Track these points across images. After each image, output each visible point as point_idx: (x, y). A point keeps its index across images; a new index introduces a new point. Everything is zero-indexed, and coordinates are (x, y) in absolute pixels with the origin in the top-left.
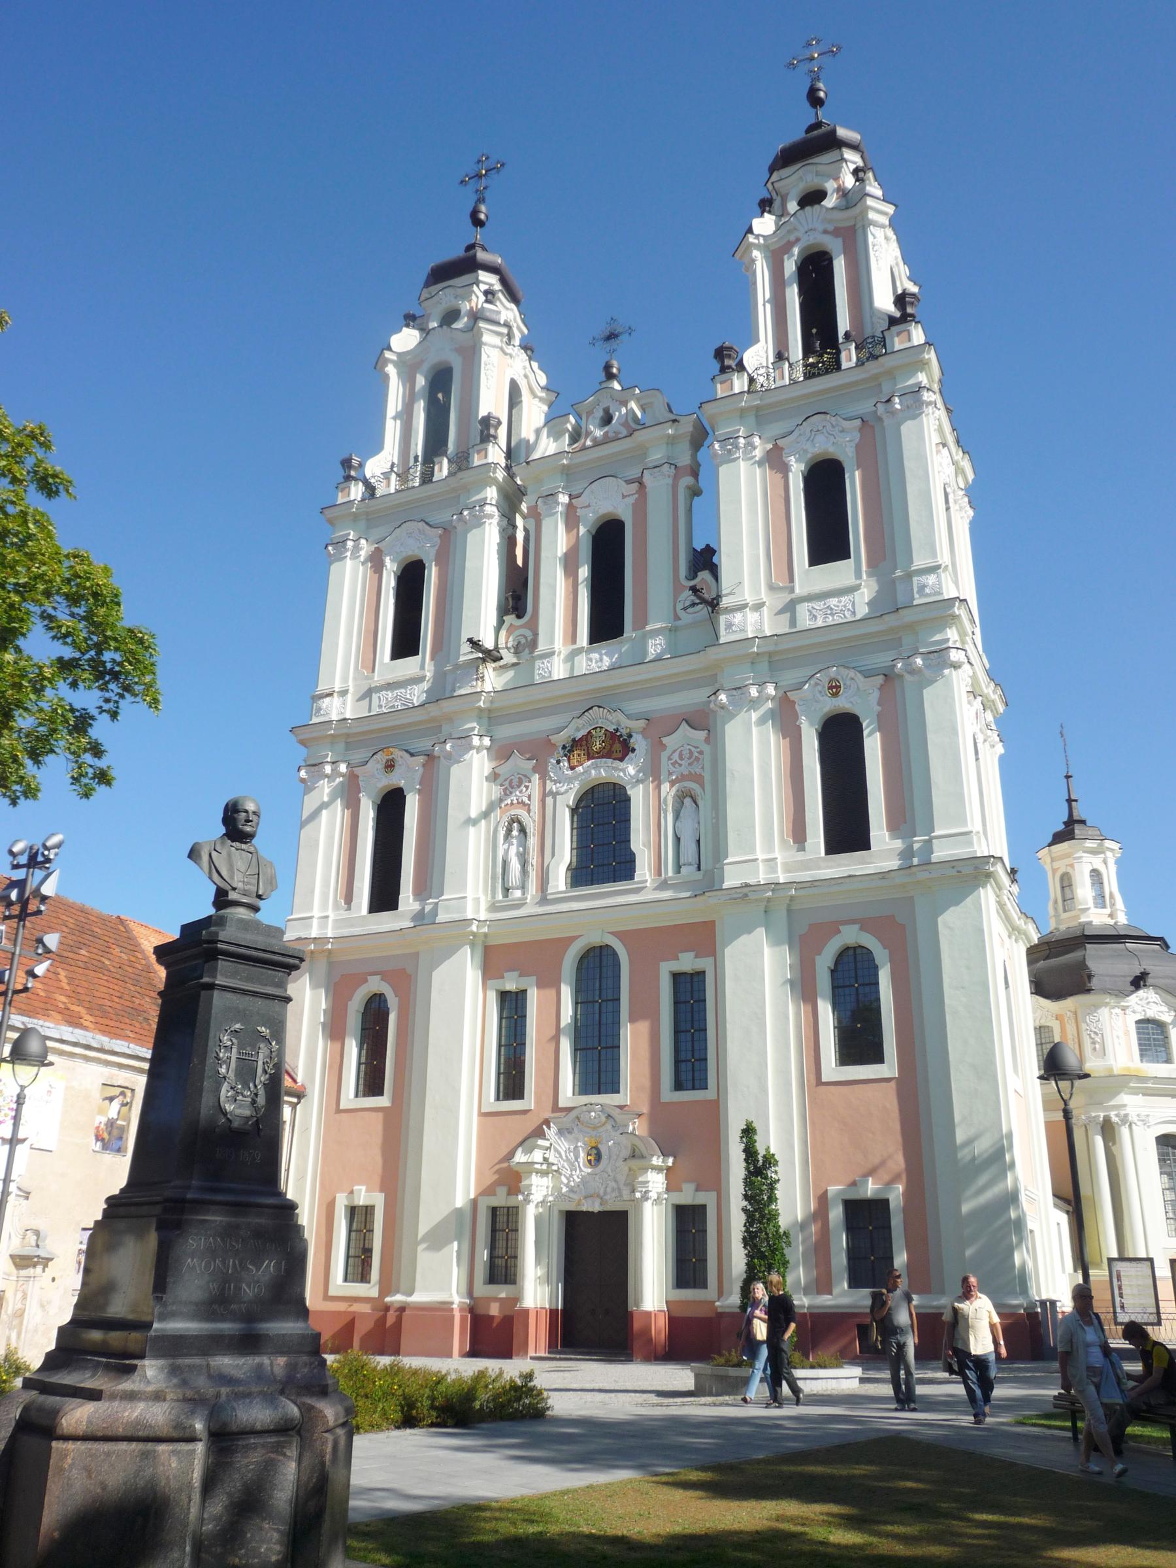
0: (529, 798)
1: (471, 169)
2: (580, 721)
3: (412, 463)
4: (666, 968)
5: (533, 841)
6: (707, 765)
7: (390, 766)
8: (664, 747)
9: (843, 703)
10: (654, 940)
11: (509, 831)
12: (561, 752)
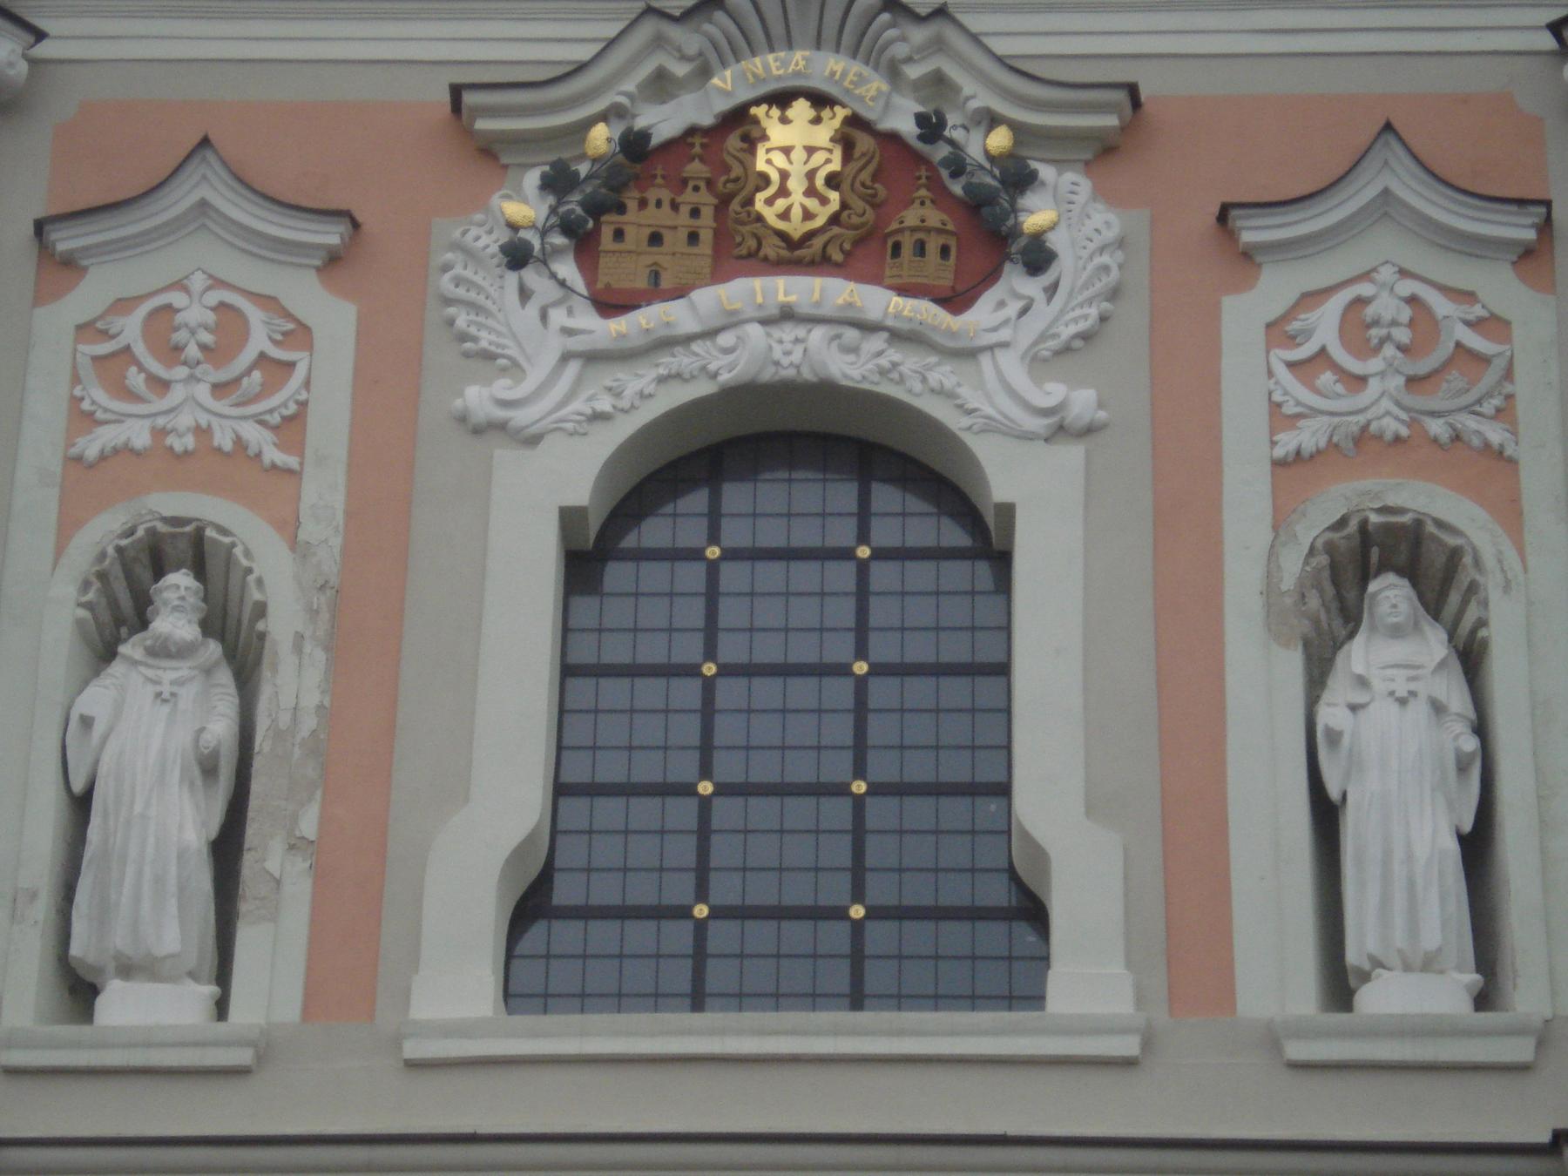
0: (291, 428)
2: (689, 39)
5: (295, 686)
12: (524, 205)
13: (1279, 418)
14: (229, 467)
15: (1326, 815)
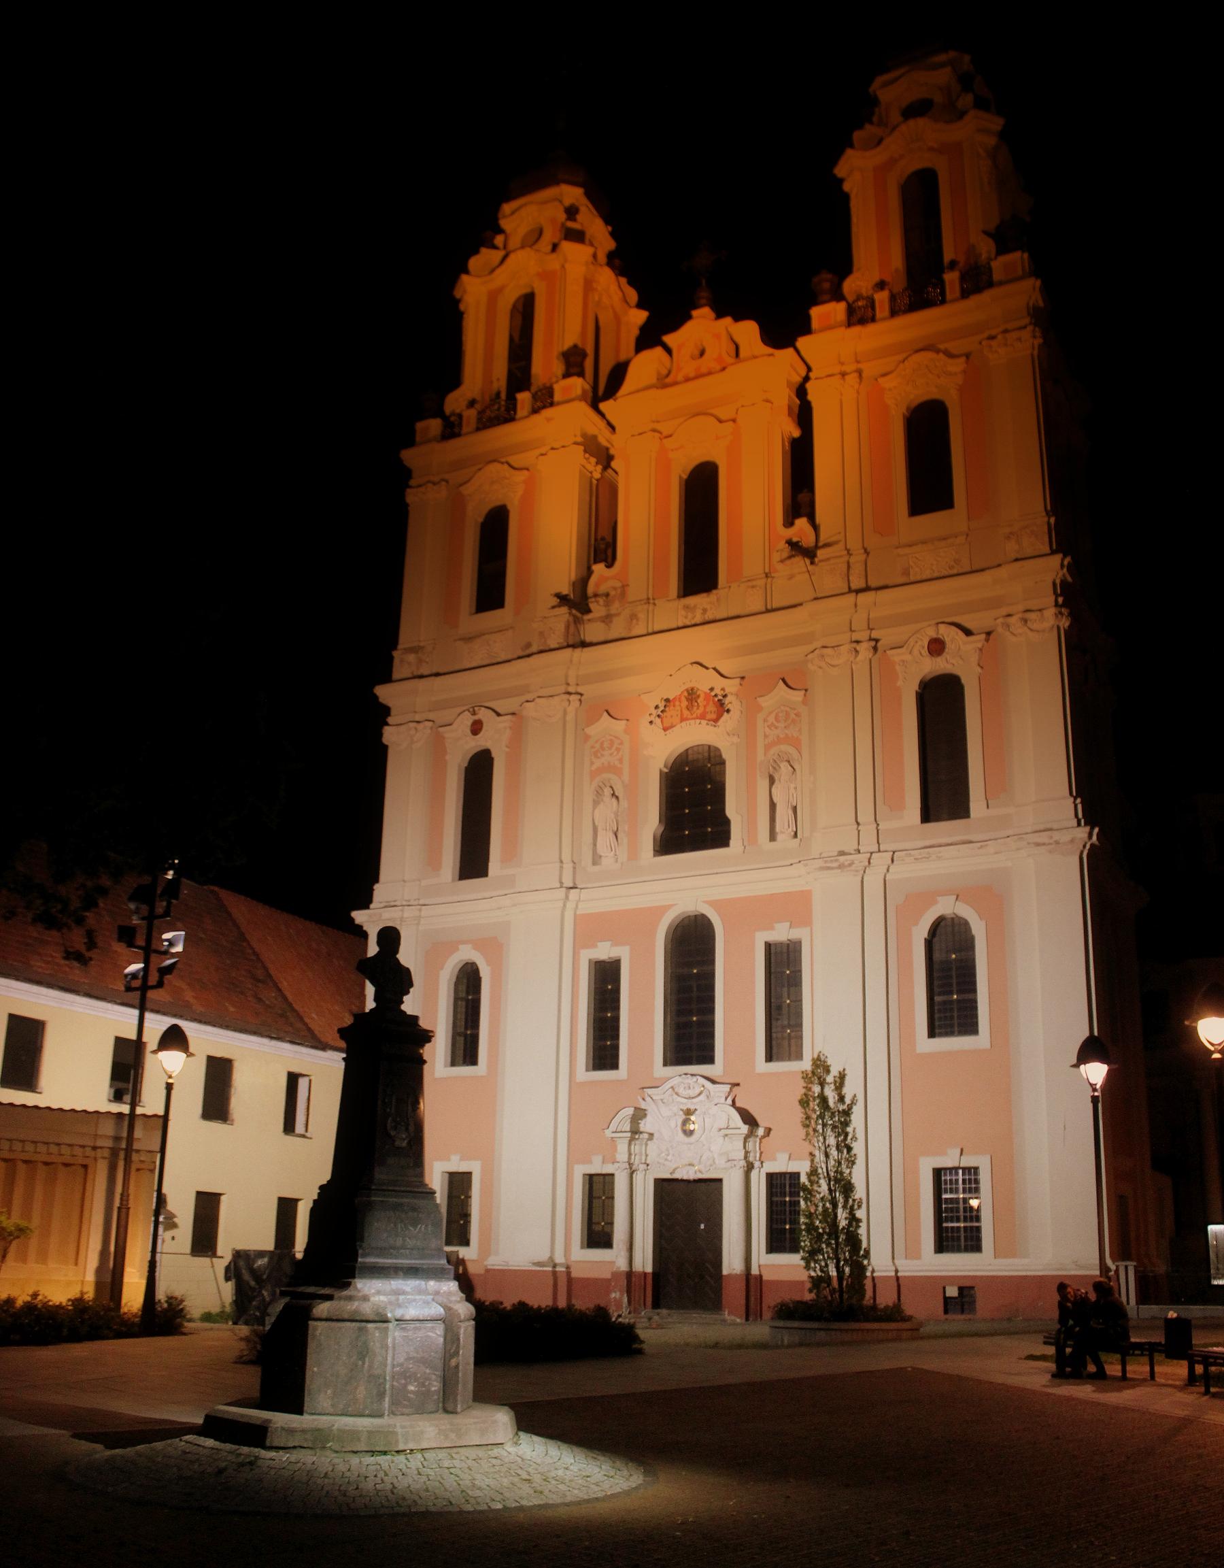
0: (621, 760)
4: (762, 938)
5: (624, 803)
7: (476, 728)
8: (760, 709)
13: (766, 736)
14: (610, 768)
15: (773, 806)
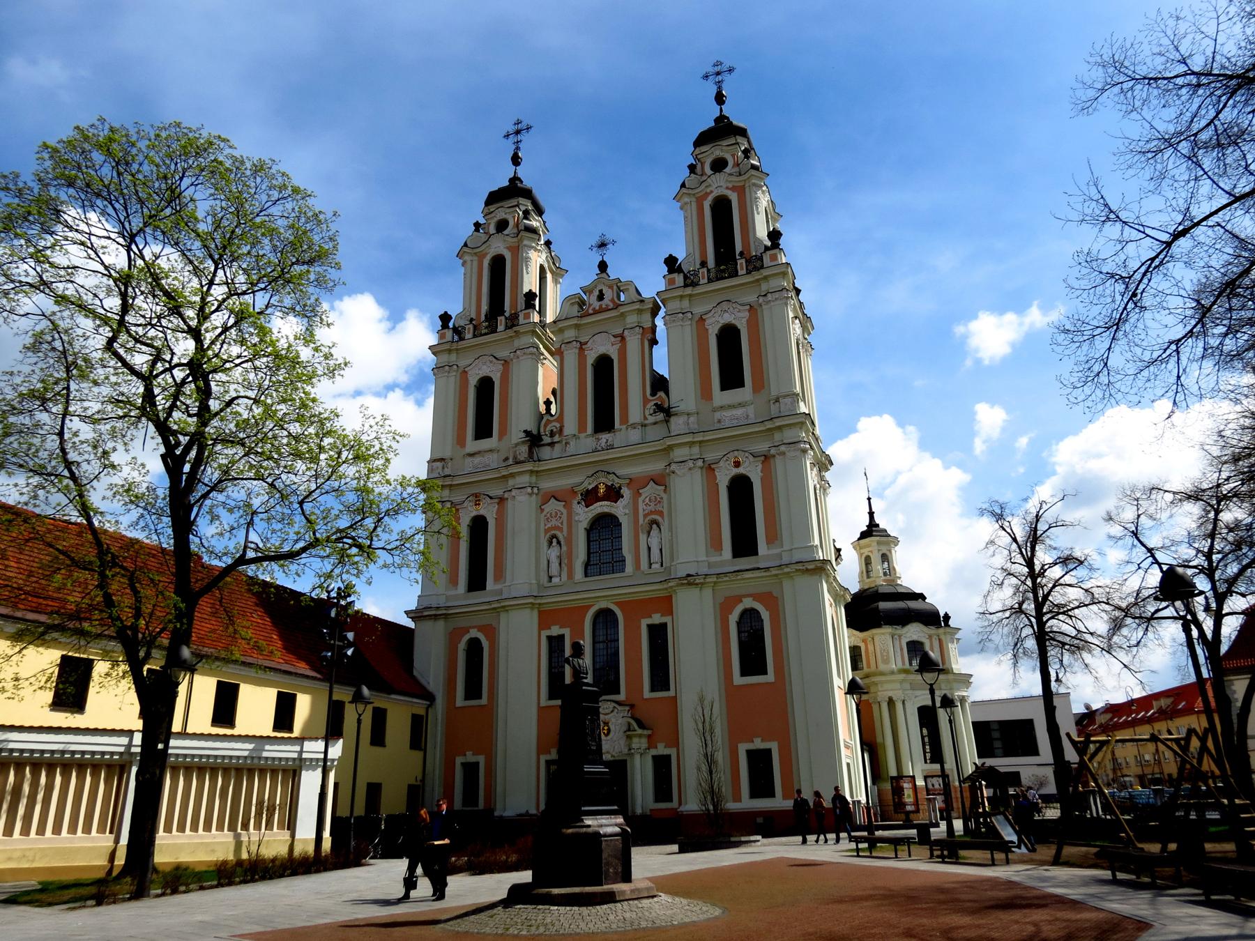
1: (512, 129)
3: (483, 318)
4: (645, 623)
5: (564, 548)
6: (665, 506)
9: (741, 470)
10: (637, 607)
11: (550, 543)
15: (649, 549)
